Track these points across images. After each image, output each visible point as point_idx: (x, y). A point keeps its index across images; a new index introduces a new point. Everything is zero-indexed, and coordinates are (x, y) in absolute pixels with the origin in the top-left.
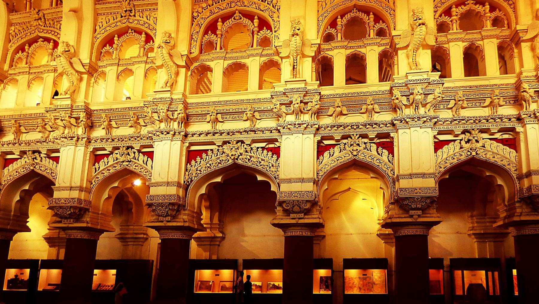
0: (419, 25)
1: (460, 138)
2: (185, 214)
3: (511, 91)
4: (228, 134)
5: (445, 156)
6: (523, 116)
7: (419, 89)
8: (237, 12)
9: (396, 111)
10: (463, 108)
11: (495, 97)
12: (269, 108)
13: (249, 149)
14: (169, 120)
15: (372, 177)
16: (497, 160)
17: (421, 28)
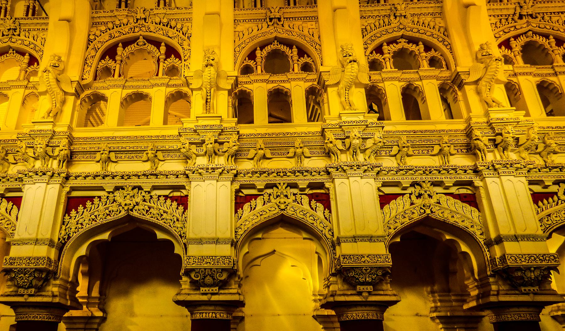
0: (350, 62)
2: (55, 285)
3: (462, 138)
4: (122, 178)
6: (481, 168)
7: (355, 132)
8: (141, 37)
9: (330, 157)
10: (408, 156)
11: (445, 145)
12: (175, 147)
13: (147, 197)
14: (48, 157)
15: (304, 239)
16: (457, 220)
17: (353, 66)
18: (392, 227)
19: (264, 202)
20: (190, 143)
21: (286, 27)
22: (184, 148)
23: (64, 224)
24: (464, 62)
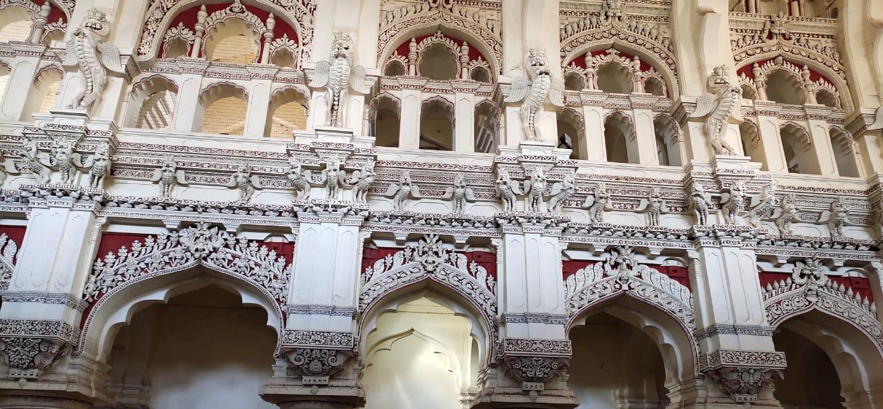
1: (602, 258)
2: (73, 366)
3: (678, 192)
5: (580, 288)
6: (698, 234)
7: (539, 172)
9: (501, 203)
10: (606, 210)
11: (655, 199)
12: (280, 171)
13: (231, 241)
14: (74, 168)
16: (662, 301)
17: (544, 79)
18: (576, 305)
19: (405, 259)
20: (302, 166)
21: (456, 13)
22: (294, 173)
23: (93, 274)
24: (691, 90)
